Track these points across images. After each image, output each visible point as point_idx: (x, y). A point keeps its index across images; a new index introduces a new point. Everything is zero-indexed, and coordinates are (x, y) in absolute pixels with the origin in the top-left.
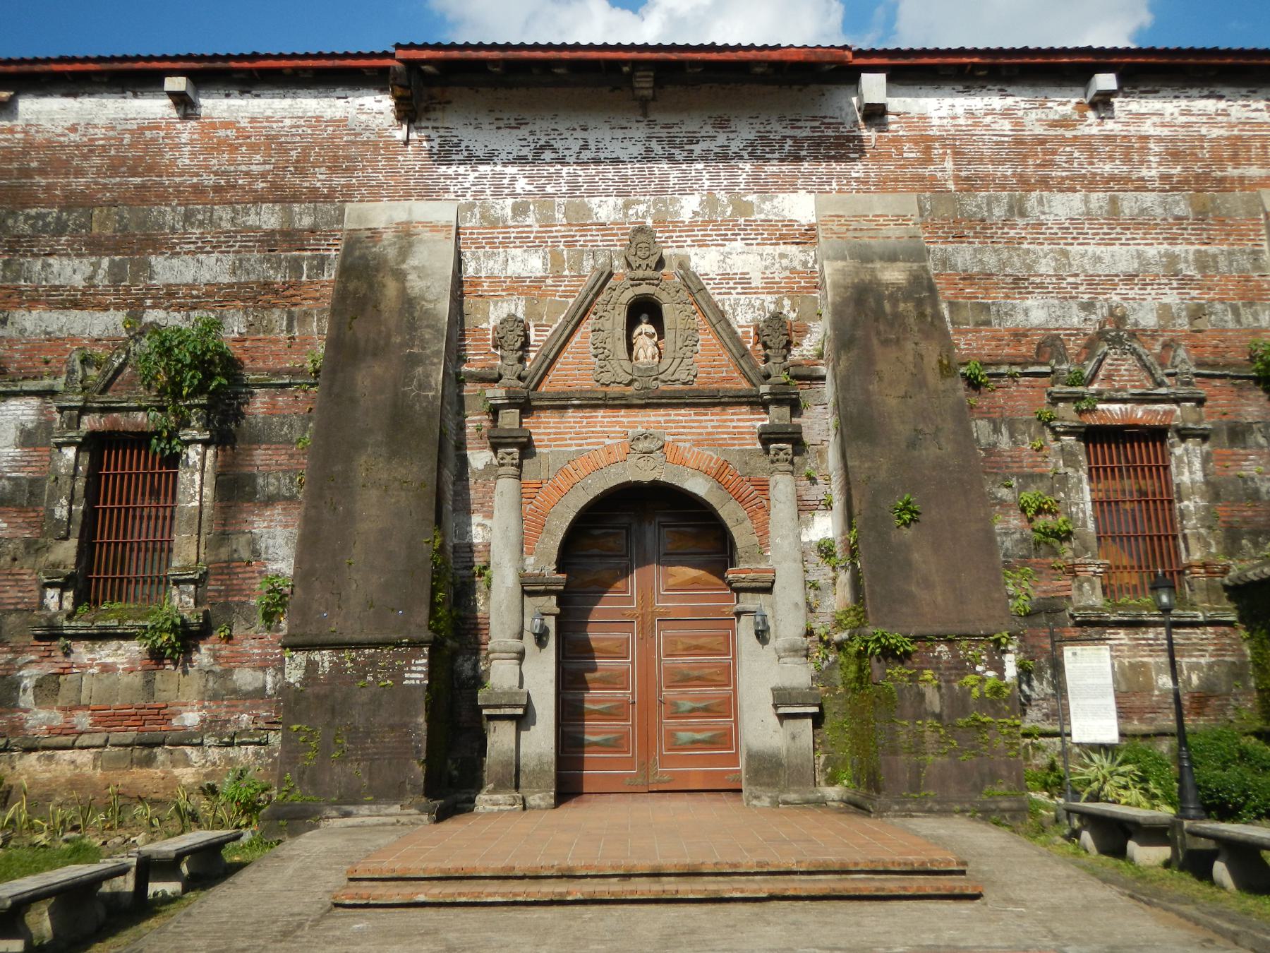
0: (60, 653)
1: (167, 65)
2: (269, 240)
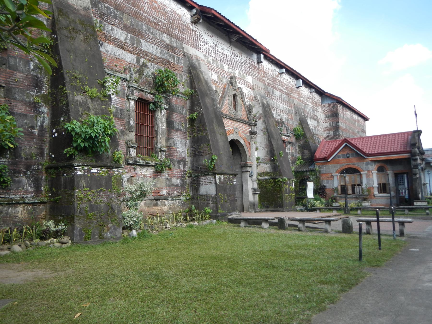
0: (133, 170)
2: (167, 47)
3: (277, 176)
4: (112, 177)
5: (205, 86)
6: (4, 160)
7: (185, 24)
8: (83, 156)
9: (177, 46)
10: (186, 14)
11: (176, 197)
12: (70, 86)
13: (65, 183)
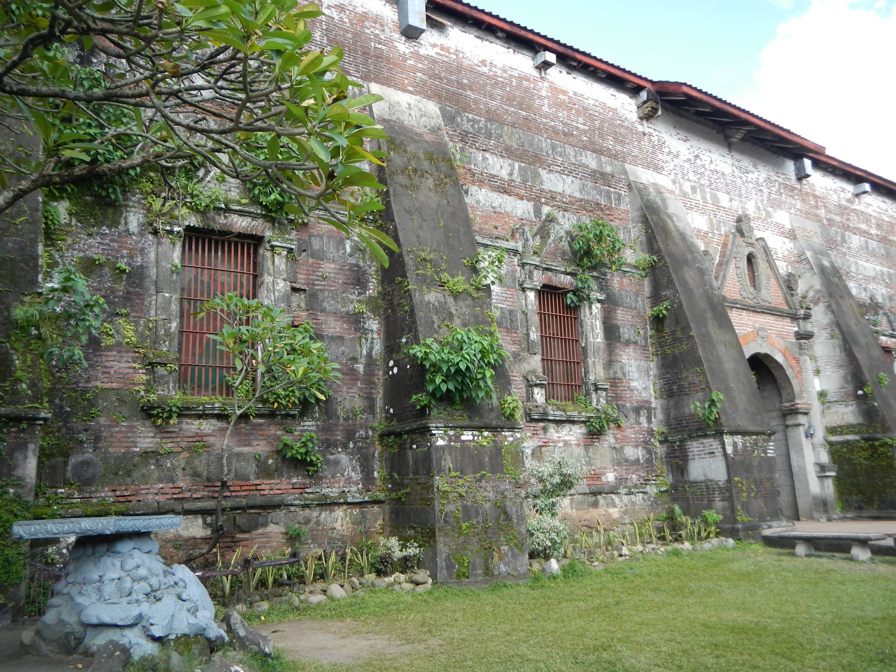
0: (542, 432)
1: (550, 44)
3: (877, 432)
4: (501, 448)
5: (681, 244)
6: (310, 423)
7: (626, 124)
8: (444, 409)
9: (613, 172)
10: (627, 106)
11: (635, 486)
12: (414, 276)
13: (416, 462)
